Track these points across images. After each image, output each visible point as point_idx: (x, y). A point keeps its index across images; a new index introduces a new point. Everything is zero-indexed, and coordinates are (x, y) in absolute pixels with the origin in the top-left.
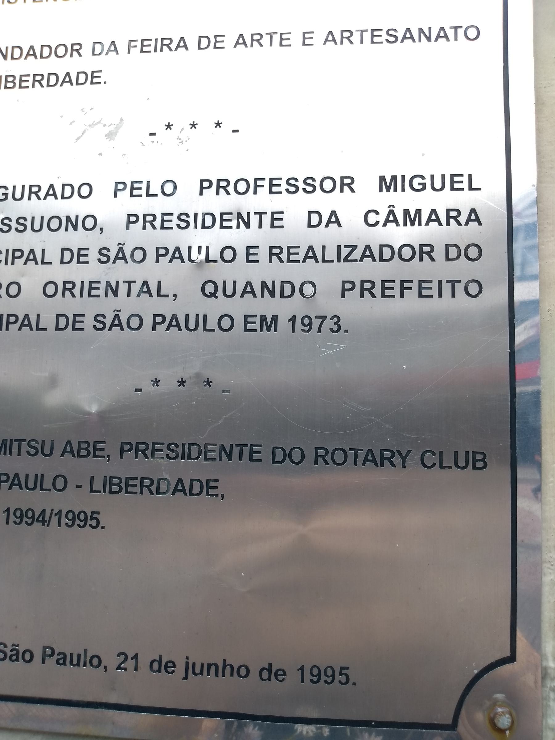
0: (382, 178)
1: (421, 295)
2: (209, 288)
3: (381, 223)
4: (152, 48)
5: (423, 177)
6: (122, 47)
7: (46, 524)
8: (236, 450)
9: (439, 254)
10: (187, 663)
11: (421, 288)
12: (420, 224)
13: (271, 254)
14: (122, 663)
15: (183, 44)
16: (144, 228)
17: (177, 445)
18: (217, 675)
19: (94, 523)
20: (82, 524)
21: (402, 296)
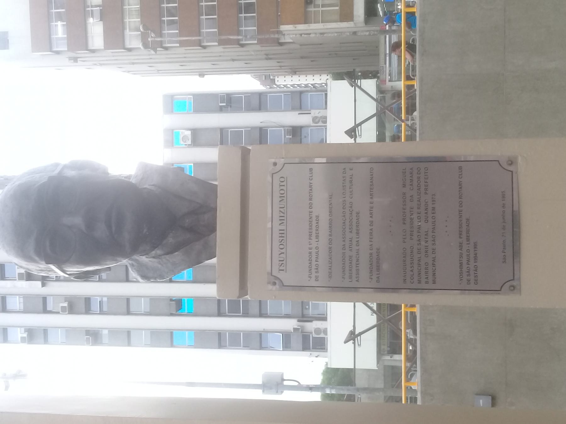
1: (427, 179)
5: (403, 179)
6: (371, 243)
8: (460, 215)
11: (426, 179)
15: (371, 230)
21: (427, 182)
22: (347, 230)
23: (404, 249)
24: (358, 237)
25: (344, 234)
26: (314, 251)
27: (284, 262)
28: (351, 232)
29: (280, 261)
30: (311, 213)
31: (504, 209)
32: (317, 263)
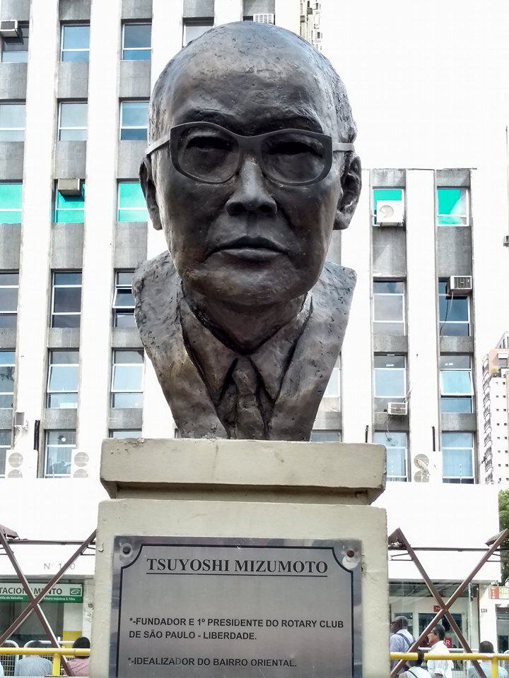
26: (187, 629)
29: (169, 561)
30: (259, 623)
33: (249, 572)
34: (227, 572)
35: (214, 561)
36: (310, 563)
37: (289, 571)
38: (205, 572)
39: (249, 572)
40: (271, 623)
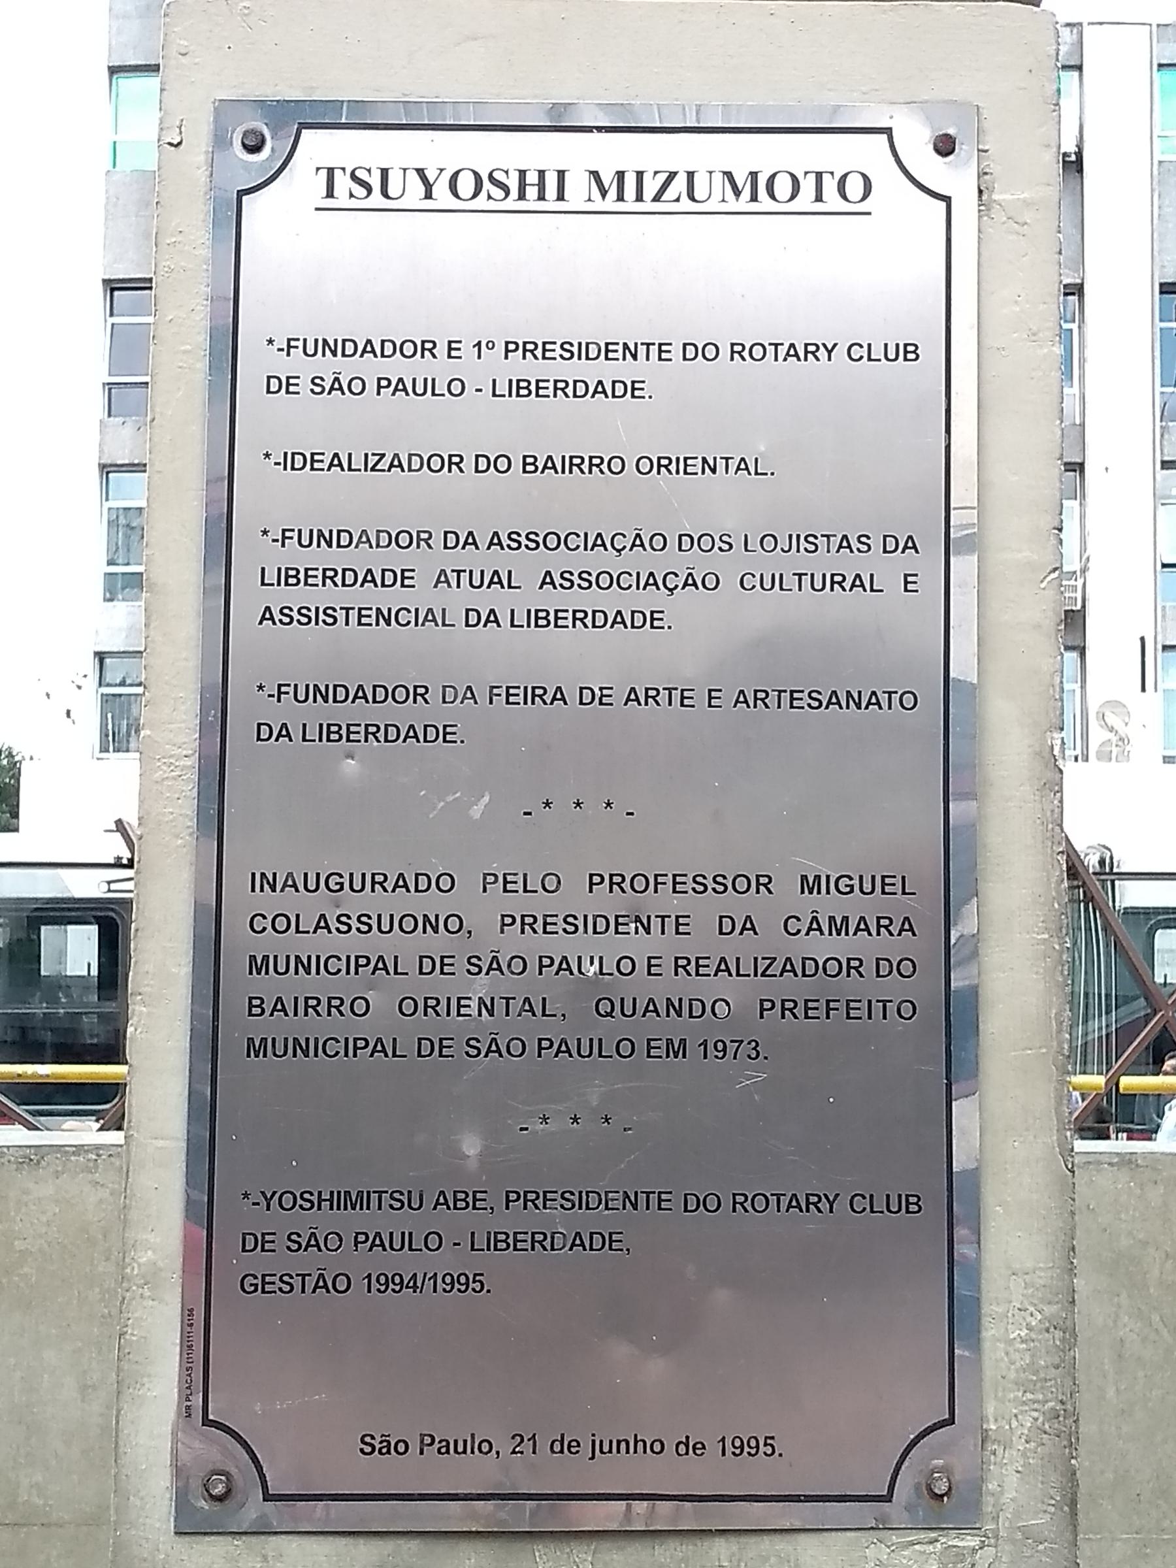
0: (804, 878)
2: (605, 1007)
3: (803, 932)
4: (521, 699)
5: (851, 879)
6: (482, 695)
7: (418, 1290)
8: (642, 1198)
9: (869, 969)
10: (594, 1442)
12: (847, 934)
13: (677, 966)
14: (518, 1445)
15: (559, 695)
16: (523, 932)
17: (572, 1194)
18: (628, 1452)
19: (478, 1286)
20: (463, 1288)
21: (828, 1017)
22: (559, 560)
23: (445, 883)
24: (521, 619)
25: (535, 542)
26: (439, 368)
27: (377, 200)
28: (548, 579)
29: (385, 173)
31: (670, 1447)
32: (372, 386)
33: (630, 204)
34: (561, 206)
35: (522, 173)
36: (819, 176)
37: (754, 198)
38: (492, 205)
39: (630, 204)
40: (694, 351)
